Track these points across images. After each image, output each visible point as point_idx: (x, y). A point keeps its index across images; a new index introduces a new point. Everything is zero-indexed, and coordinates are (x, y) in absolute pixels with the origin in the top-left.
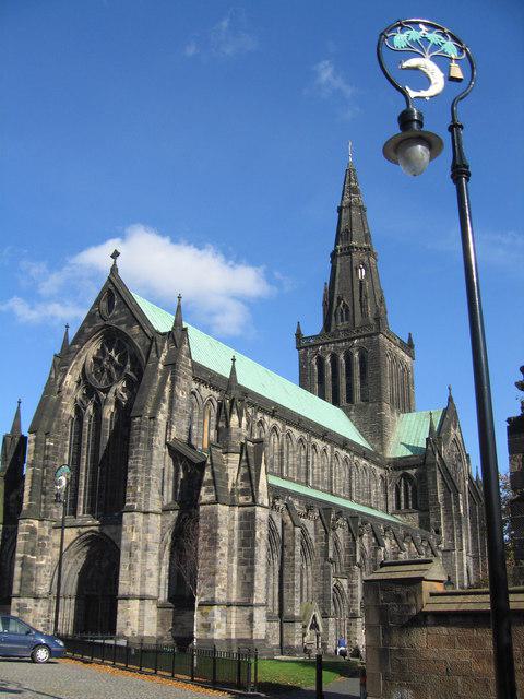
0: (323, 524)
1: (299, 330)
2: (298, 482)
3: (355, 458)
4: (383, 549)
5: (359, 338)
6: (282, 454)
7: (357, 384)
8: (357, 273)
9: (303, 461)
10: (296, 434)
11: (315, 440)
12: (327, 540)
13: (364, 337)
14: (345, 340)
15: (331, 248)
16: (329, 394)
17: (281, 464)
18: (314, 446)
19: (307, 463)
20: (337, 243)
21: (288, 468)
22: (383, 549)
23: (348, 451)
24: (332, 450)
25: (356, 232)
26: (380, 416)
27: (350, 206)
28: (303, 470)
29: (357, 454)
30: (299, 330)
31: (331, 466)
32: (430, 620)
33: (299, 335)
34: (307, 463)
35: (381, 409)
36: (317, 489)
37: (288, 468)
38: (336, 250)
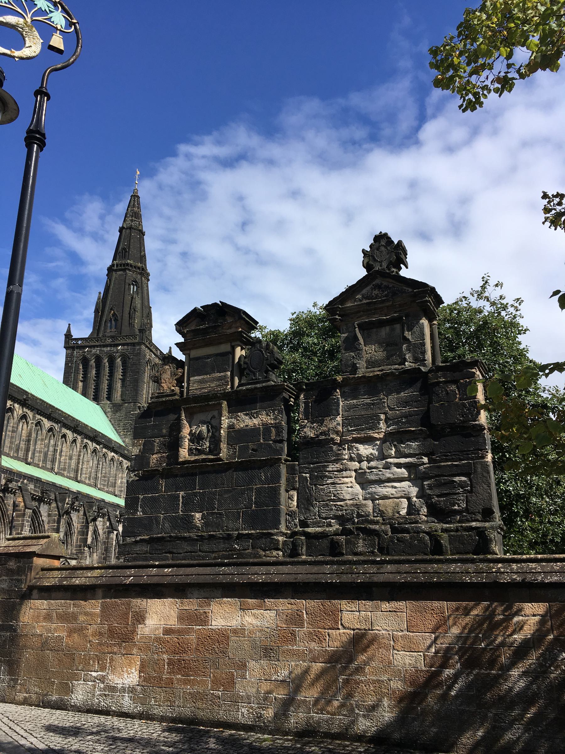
0: (58, 507)
1: (69, 330)
2: (43, 468)
3: (104, 450)
4: (115, 532)
5: (123, 345)
6: (29, 441)
7: (119, 385)
8: (130, 289)
9: (51, 449)
10: (47, 424)
11: (64, 431)
12: (59, 522)
13: (127, 344)
14: (111, 346)
15: (109, 262)
16: (91, 392)
17: (27, 450)
18: (64, 436)
19: (55, 451)
20: (114, 259)
21: (33, 454)
22: (115, 532)
23: (98, 443)
24: (82, 441)
25: (133, 251)
27: (130, 228)
28: (50, 456)
29: (106, 447)
30: (69, 330)
31: (79, 456)
32: (35, 592)
33: (68, 336)
34: (55, 451)
36: (63, 475)
37: (33, 454)
38: (113, 265)
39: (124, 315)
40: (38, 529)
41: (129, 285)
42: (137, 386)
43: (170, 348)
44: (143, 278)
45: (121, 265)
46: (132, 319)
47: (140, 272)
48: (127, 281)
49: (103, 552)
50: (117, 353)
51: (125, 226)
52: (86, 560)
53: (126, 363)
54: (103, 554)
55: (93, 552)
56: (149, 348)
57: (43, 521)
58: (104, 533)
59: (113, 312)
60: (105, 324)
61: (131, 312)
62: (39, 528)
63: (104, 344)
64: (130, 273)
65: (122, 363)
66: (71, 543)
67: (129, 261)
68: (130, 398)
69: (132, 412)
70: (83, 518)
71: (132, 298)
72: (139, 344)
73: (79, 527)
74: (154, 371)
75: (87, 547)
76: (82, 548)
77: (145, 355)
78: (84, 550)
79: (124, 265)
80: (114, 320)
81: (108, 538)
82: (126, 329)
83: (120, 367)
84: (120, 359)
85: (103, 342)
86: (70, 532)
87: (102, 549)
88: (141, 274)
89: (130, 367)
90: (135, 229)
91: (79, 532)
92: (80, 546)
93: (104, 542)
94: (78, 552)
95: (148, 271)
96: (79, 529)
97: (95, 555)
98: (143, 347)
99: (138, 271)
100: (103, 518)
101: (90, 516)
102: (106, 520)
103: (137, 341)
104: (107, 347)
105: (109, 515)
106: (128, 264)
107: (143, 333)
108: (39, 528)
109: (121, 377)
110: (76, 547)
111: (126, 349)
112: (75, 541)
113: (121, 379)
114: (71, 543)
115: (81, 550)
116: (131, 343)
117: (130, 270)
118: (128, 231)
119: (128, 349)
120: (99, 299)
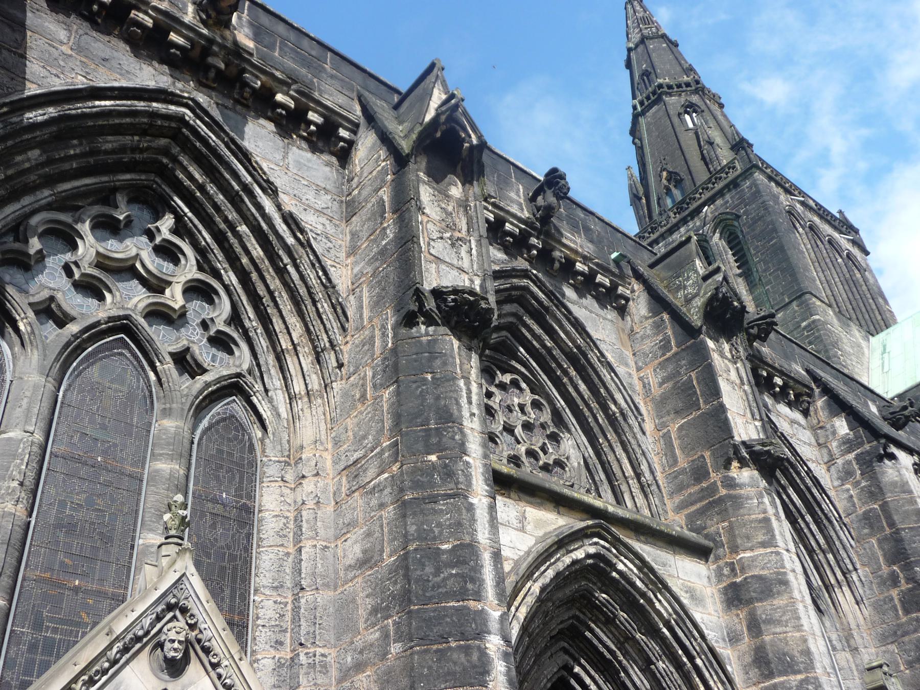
5: (711, 201)
8: (683, 122)
13: (720, 193)
14: (684, 221)
26: (813, 326)
35: (808, 311)
39: (691, 164)
40: (275, 284)
41: (679, 114)
42: (787, 259)
43: (840, 212)
44: (708, 102)
45: (648, 98)
46: (712, 163)
47: (693, 88)
48: (671, 112)
49: (885, 570)
50: (705, 225)
51: (631, 45)
52: (770, 542)
53: (737, 237)
54: (894, 580)
55: (828, 587)
56: (778, 184)
57: (290, 220)
58: (846, 474)
59: (665, 174)
60: (659, 203)
61: (705, 152)
62: (281, 272)
63: (669, 226)
64: (673, 98)
65: (729, 243)
66: (638, 475)
67: (660, 81)
68: (783, 294)
69: (804, 324)
70: (658, 327)
71: (697, 134)
72: (747, 173)
73: (653, 380)
74: (819, 243)
75: (743, 463)
76: (715, 477)
77: (776, 198)
78: (730, 483)
79: (654, 93)
80: (675, 186)
81: (875, 491)
82: (702, 175)
83: (726, 252)
84: (717, 235)
85: (665, 226)
86: (605, 408)
87: (870, 560)
88: (696, 92)
89: (748, 233)
90: (651, 38)
91: (660, 404)
92: (699, 473)
93: (868, 519)
94: (702, 512)
95: (713, 91)
96: (656, 391)
97: (844, 598)
98: (758, 176)
99: (689, 89)
100: (806, 413)
101: (688, 301)
102: (823, 415)
103: (739, 171)
104: (679, 228)
105: (827, 390)
106: (660, 86)
107: (744, 148)
108: (281, 272)
109: (739, 271)
110: (680, 488)
111: (722, 205)
112: (652, 457)
113: (740, 275)
114: (638, 475)
115: (713, 489)
116: (727, 186)
117: (670, 95)
118: (640, 49)
119: (728, 202)
120: (631, 177)
